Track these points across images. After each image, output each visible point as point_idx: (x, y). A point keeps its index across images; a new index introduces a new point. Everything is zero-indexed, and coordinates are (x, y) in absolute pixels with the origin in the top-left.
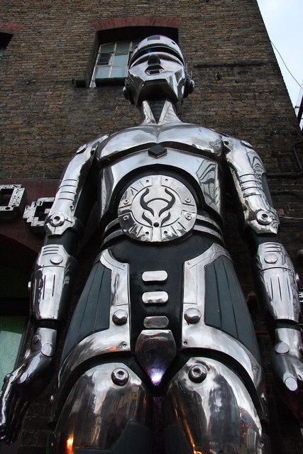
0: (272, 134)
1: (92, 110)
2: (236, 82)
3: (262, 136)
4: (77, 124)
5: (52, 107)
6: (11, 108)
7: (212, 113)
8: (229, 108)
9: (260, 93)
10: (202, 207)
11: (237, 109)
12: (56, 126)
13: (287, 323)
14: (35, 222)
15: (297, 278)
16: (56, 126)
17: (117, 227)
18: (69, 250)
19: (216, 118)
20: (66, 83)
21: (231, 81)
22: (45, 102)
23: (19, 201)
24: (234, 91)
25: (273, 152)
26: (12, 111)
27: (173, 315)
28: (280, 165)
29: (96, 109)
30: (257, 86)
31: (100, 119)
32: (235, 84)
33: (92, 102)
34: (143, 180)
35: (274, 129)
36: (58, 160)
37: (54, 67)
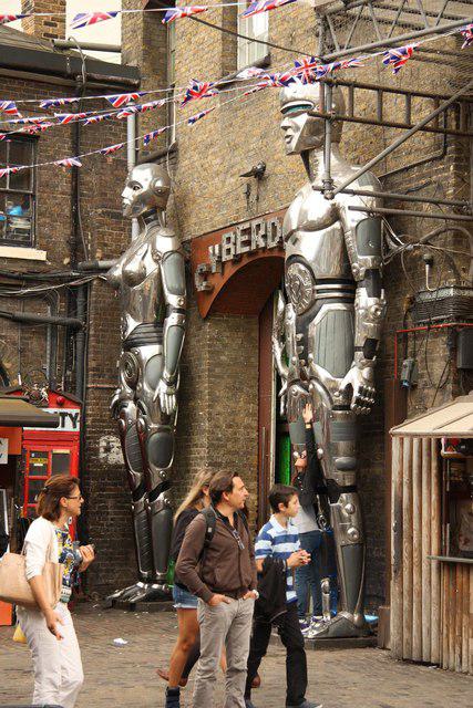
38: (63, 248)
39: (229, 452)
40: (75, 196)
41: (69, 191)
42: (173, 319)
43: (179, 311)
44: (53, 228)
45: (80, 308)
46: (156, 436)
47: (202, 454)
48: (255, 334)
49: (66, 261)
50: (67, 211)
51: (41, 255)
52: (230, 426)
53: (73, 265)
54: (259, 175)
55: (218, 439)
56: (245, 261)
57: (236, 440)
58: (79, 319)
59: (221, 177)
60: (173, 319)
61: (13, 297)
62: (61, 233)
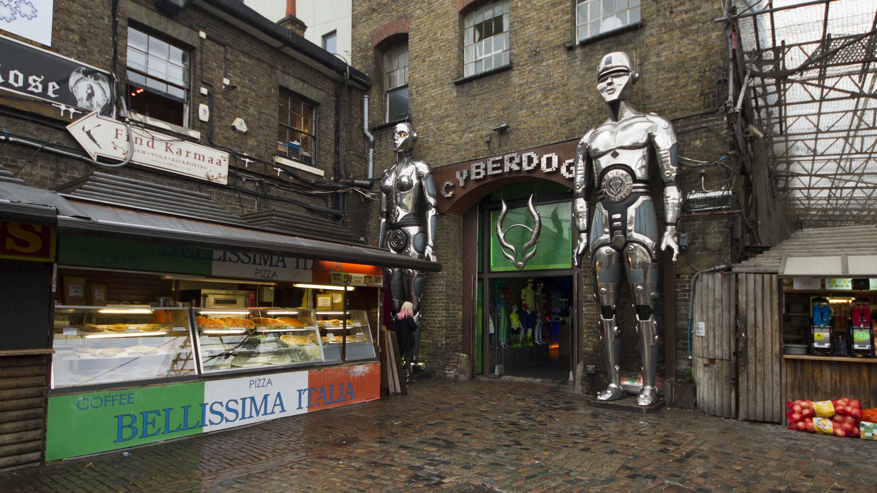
0: (705, 71)
1: (581, 73)
2: (686, 13)
3: (697, 76)
4: (575, 90)
5: (557, 75)
6: (533, 83)
7: (663, 58)
8: (676, 50)
9: (703, 23)
10: (635, 180)
11: (682, 49)
12: (562, 94)
13: (671, 224)
14: (567, 175)
15: (693, 192)
16: (562, 94)
17: (601, 194)
18: (586, 200)
19: (666, 64)
20: (559, 46)
21: (681, 12)
22: (550, 72)
23: (557, 164)
24: (684, 25)
25: (702, 91)
26: (533, 86)
27: (624, 230)
28: (704, 102)
29: (584, 72)
30: (704, 14)
31: (588, 82)
32: (684, 16)
33: (581, 65)
34: (609, 174)
35: (706, 66)
36: (569, 124)
37: (548, 28)
38: (331, 170)
39: (453, 289)
40: (337, 143)
41: (334, 139)
42: (432, 213)
43: (435, 207)
44: (326, 158)
45: (341, 206)
46: (418, 280)
47: (440, 289)
48: (462, 225)
49: (332, 178)
50: (333, 150)
51: (321, 173)
52: (453, 275)
53: (336, 181)
54: (502, 131)
55: (449, 282)
56: (489, 180)
57: (455, 282)
58: (340, 212)
59: (459, 134)
60: (432, 213)
61: (309, 195)
62: (330, 162)
